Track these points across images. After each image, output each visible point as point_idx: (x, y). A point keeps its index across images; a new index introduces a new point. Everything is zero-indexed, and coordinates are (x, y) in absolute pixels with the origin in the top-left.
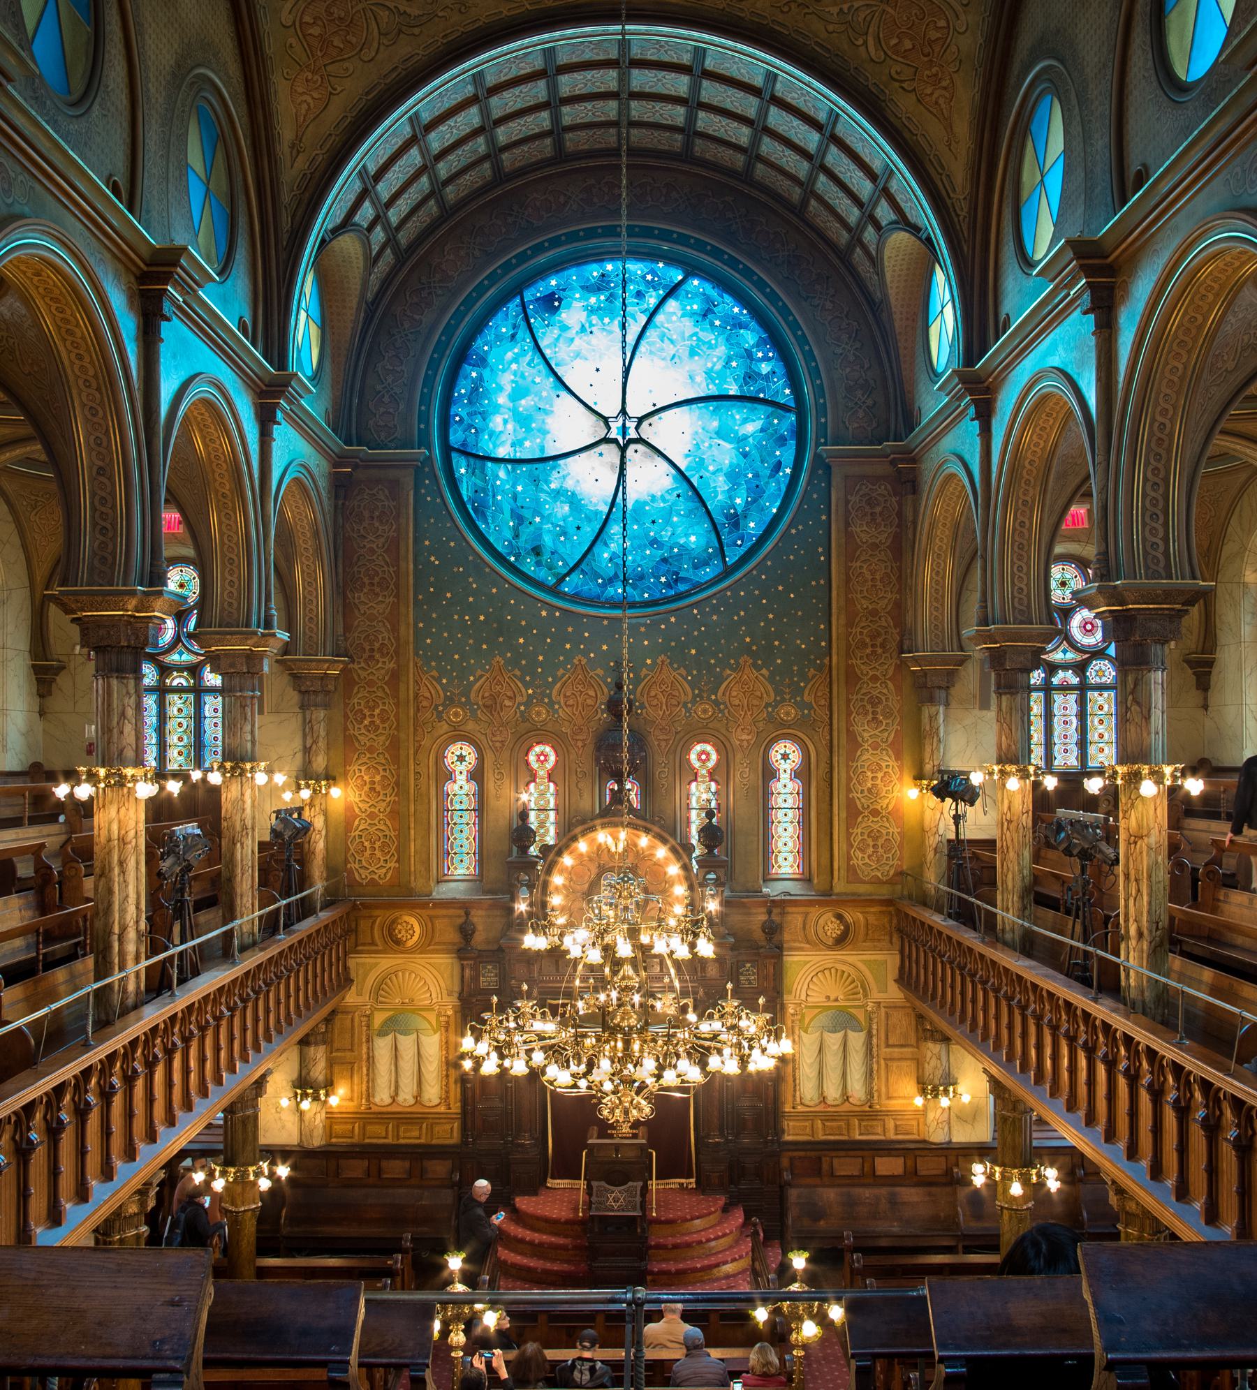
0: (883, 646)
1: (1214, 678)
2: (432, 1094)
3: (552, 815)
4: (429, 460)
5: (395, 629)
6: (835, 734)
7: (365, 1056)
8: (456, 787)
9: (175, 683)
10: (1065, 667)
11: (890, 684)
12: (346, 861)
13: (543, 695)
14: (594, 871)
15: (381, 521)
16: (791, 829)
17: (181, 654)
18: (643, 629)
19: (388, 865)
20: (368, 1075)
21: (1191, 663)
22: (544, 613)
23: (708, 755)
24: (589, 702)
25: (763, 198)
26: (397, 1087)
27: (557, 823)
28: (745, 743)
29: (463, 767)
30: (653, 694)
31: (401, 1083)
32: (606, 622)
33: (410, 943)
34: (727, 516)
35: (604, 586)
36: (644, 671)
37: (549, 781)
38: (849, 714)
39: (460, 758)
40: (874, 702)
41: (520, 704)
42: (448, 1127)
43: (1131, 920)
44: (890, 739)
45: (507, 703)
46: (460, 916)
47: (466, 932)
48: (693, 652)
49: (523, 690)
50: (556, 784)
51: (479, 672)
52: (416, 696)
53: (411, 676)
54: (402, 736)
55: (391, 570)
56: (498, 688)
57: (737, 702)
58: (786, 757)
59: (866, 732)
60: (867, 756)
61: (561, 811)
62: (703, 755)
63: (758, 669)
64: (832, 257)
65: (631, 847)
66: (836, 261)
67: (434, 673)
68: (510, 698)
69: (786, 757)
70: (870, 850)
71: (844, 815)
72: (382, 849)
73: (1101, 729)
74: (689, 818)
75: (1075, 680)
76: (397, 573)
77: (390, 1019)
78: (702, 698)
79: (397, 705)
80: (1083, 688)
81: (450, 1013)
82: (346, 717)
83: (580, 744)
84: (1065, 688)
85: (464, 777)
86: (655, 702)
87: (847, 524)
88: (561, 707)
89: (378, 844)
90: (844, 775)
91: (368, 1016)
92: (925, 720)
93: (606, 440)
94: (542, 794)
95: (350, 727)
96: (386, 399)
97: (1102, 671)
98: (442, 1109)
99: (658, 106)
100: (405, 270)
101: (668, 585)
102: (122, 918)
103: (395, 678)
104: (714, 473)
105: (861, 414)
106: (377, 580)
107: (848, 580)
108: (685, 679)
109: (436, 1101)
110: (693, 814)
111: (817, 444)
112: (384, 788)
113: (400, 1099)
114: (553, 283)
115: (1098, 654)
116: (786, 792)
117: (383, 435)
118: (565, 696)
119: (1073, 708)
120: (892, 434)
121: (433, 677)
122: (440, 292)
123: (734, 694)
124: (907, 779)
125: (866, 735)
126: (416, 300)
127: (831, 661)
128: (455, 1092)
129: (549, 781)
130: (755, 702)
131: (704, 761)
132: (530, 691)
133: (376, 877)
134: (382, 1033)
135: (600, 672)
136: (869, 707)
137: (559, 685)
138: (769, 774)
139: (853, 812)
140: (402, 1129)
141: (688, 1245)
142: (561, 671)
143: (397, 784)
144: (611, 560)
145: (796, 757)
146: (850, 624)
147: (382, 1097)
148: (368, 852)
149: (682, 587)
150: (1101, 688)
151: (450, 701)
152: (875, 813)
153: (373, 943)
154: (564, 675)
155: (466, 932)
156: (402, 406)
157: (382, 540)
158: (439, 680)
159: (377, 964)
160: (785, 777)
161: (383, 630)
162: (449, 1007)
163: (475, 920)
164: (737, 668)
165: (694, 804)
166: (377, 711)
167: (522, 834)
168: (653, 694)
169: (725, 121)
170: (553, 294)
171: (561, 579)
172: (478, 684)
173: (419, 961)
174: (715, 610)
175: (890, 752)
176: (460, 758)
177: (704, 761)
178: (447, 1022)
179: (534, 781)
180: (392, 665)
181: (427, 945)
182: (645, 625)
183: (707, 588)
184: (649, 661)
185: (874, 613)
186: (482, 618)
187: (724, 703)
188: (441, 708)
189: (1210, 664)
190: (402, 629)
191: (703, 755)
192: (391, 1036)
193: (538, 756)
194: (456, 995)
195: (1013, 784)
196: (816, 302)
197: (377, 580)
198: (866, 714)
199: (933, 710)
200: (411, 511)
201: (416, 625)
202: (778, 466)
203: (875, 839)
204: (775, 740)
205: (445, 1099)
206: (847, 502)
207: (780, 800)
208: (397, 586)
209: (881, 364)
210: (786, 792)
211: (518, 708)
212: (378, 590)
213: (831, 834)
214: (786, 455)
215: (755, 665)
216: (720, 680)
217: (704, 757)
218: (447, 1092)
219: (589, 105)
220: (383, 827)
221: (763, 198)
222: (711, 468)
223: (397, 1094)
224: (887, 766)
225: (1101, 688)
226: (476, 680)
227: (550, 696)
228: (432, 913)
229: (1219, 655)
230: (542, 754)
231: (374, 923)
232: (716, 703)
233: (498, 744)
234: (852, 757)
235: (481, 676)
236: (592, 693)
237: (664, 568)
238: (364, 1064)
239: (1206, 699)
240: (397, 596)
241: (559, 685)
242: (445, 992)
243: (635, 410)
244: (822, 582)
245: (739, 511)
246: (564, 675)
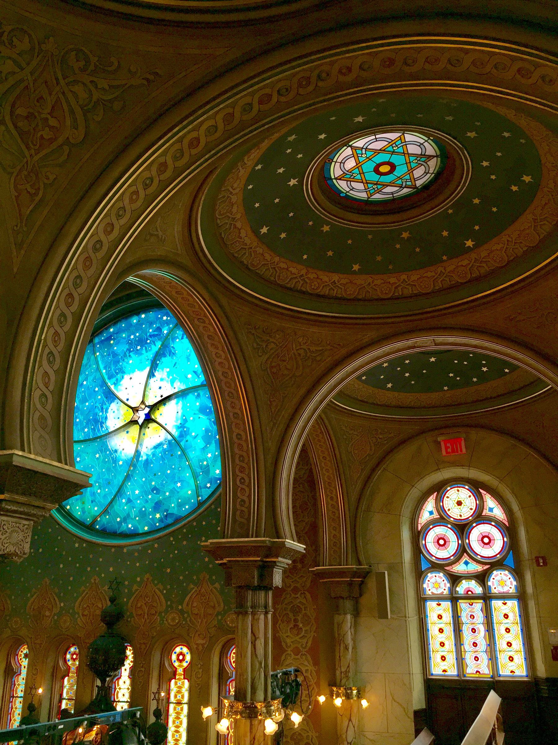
10: (469, 577)
11: (308, 595)
18: (136, 554)
30: (139, 605)
32: (113, 550)
34: (201, 467)
35: (120, 523)
36: (135, 587)
40: (296, 610)
41: (55, 615)
44: (309, 644)
45: (47, 613)
49: (58, 603)
57: (196, 611)
73: (509, 637)
75: (478, 590)
78: (172, 608)
80: (487, 598)
84: (470, 597)
86: (140, 612)
93: (134, 422)
97: (502, 581)
101: (161, 520)
104: (195, 437)
114: (112, 330)
115: (496, 564)
119: (480, 617)
123: (195, 604)
124: (324, 684)
125: (288, 641)
131: (181, 661)
136: (291, 615)
137: (80, 599)
142: (83, 588)
144: (127, 503)
149: (170, 521)
150: (504, 597)
154: (84, 591)
168: (139, 605)
172: (32, 599)
175: (309, 658)
177: (181, 661)
182: (138, 551)
187: (187, 612)
198: (288, 622)
199: (341, 617)
211: (53, 618)
222: (193, 434)
224: (307, 671)
225: (504, 597)
226: (32, 596)
232: (182, 612)
233: (38, 646)
235: (35, 593)
241: (80, 599)
243: (151, 401)
245: (210, 462)
246: (84, 591)
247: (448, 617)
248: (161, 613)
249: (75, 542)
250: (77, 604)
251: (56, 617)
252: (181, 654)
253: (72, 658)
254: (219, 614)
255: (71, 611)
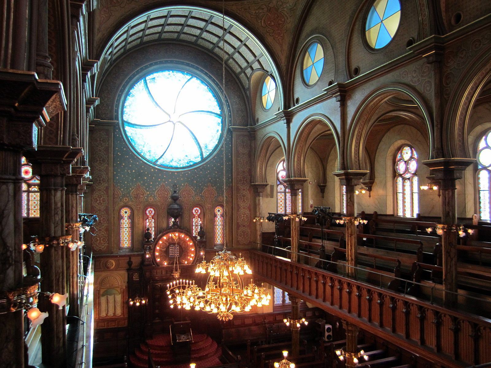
0: (246, 181)
1: (326, 190)
2: (119, 312)
3: (153, 228)
4: (118, 123)
5: (107, 174)
6: (234, 205)
7: (97, 303)
8: (124, 221)
9: (33, 190)
11: (248, 191)
12: (92, 244)
13: (152, 194)
14: (167, 244)
15: (103, 142)
16: (220, 231)
17: (35, 180)
19: (105, 245)
20: (99, 308)
21: (320, 186)
22: (152, 170)
23: (198, 211)
24: (166, 196)
25: (215, 57)
26: (108, 311)
27: (155, 231)
28: (209, 208)
29: (126, 215)
31: (109, 310)
33: (112, 268)
37: (152, 218)
38: (237, 199)
39: (125, 213)
42: (123, 322)
43: (349, 256)
45: (141, 196)
46: (127, 259)
47: (130, 263)
48: (195, 182)
49: (146, 192)
50: (154, 220)
51: (133, 187)
52: (113, 194)
53: (112, 188)
54: (110, 206)
55: (106, 156)
56: (139, 192)
58: (219, 211)
59: (242, 204)
60: (242, 211)
61: (156, 228)
62: (196, 211)
63: (213, 187)
64: (233, 75)
65: (179, 238)
66: (235, 77)
67: (119, 187)
68: (142, 195)
69: (219, 211)
70: (243, 236)
71: (236, 227)
72: (103, 240)
74: (193, 228)
76: (108, 157)
77: (106, 291)
78: (197, 195)
79: (108, 197)
81: (124, 288)
82: (92, 200)
83: (163, 208)
85: (127, 218)
86: (184, 196)
87: (237, 148)
88: (157, 197)
89: (102, 239)
90: (236, 215)
91: (99, 291)
92: (257, 201)
93: (169, 121)
94: (150, 223)
95: (93, 203)
96: (105, 105)
98: (122, 316)
99: (193, 29)
100: (112, 67)
102: (73, 270)
103: (107, 188)
105: (240, 118)
106: (101, 159)
107: (237, 163)
108: (193, 189)
109: (120, 314)
110: (194, 227)
111: (229, 126)
112: (103, 222)
113: (109, 315)
116: (219, 221)
117: (104, 116)
118: (158, 194)
120: (249, 124)
121: (119, 188)
122: (122, 75)
123: (206, 194)
125: (242, 205)
126: (114, 76)
127: (232, 185)
128: (126, 311)
129: (152, 218)
130: (212, 196)
131: (197, 212)
132: (148, 193)
133: (101, 249)
134: (103, 295)
135: (169, 187)
136: (242, 197)
138: (215, 216)
139: (238, 226)
140: (110, 323)
141: (201, 349)
142: (157, 187)
143: (108, 220)
145: (221, 211)
146: (238, 175)
147: (103, 314)
148: (99, 241)
149: (192, 164)
151: (124, 196)
152: (244, 226)
153: (100, 269)
155: (130, 263)
156: (110, 108)
157: (104, 147)
158: (120, 189)
159: (101, 275)
160: (219, 217)
161: (103, 174)
162: (124, 285)
163: (132, 260)
164: (207, 187)
165: (194, 224)
166: (101, 199)
167: (147, 235)
169: (211, 35)
170: (154, 78)
171: (157, 161)
172: (132, 191)
173: (115, 273)
174: (201, 170)
176: (125, 213)
178: (124, 291)
179: (148, 219)
180: (106, 185)
181: (117, 268)
183: (199, 164)
184: (183, 184)
185: (244, 172)
186: (134, 171)
187: (204, 196)
188: (121, 198)
189: (325, 186)
190: (110, 174)
191: (196, 211)
192: (106, 296)
193: (149, 211)
194: (126, 282)
195: (297, 219)
196: (229, 87)
197: (101, 159)
200: (113, 139)
201: (113, 173)
202: (218, 131)
203: (244, 233)
204: (216, 207)
205: (123, 313)
206: (237, 141)
207: (217, 223)
208: (108, 161)
209: (246, 105)
210: (219, 221)
211: (145, 197)
212: (102, 162)
213: (232, 232)
214: (220, 128)
215: (212, 186)
216: (202, 190)
217: (197, 211)
218: (123, 311)
219: (173, 27)
220: (103, 234)
221: (215, 57)
223: (108, 313)
224: (247, 213)
227: (154, 195)
228: (118, 258)
229: (328, 184)
230: (150, 211)
231: (100, 263)
232: (201, 196)
234: (238, 210)
236: (166, 193)
237: (186, 158)
238: (97, 305)
239: (323, 195)
240: (108, 164)
242: (123, 282)
244: (230, 163)
247: (283, 198)
248: (193, 197)
249: (152, 169)
250: (155, 193)
251: (146, 198)
252: (196, 210)
253: (150, 211)
254: (215, 197)
255: (153, 195)
